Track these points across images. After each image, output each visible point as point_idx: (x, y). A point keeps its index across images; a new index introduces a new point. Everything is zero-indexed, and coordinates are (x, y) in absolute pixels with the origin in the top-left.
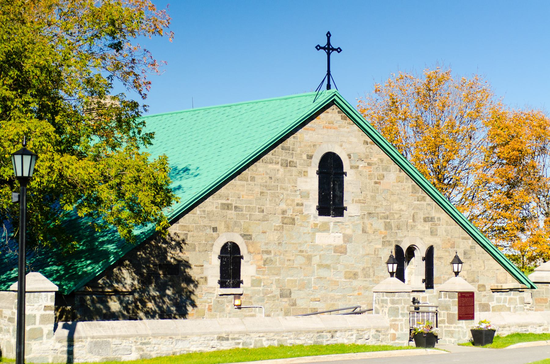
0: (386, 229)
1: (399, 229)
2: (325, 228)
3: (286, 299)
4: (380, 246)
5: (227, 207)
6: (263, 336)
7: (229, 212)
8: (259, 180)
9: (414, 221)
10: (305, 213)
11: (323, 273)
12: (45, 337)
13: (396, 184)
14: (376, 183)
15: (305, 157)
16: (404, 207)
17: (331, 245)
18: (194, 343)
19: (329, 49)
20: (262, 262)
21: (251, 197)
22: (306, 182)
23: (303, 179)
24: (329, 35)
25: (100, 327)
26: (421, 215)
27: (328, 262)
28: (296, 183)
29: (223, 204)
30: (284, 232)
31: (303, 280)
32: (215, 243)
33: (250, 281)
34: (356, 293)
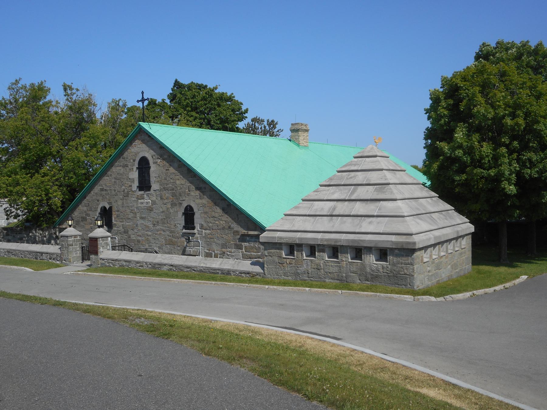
11: (142, 222)
14: (167, 170)
15: (132, 161)
23: (131, 173)
24: (143, 93)
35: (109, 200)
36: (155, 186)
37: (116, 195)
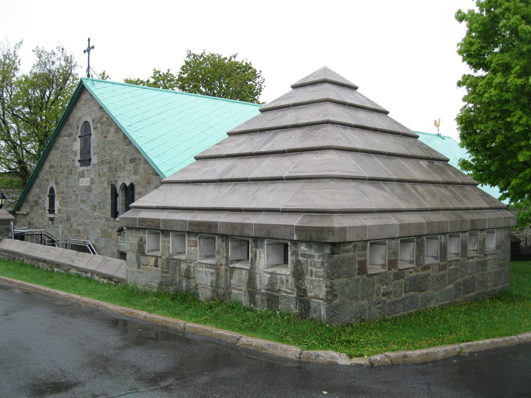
1: (116, 171)
2: (82, 175)
3: (68, 223)
8: (61, 149)
9: (124, 164)
11: (82, 206)
13: (115, 135)
15: (76, 128)
16: (119, 153)
17: (85, 186)
20: (61, 199)
24: (89, 40)
26: (128, 158)
27: (83, 199)
31: (75, 210)
35: (56, 179)
36: (94, 160)
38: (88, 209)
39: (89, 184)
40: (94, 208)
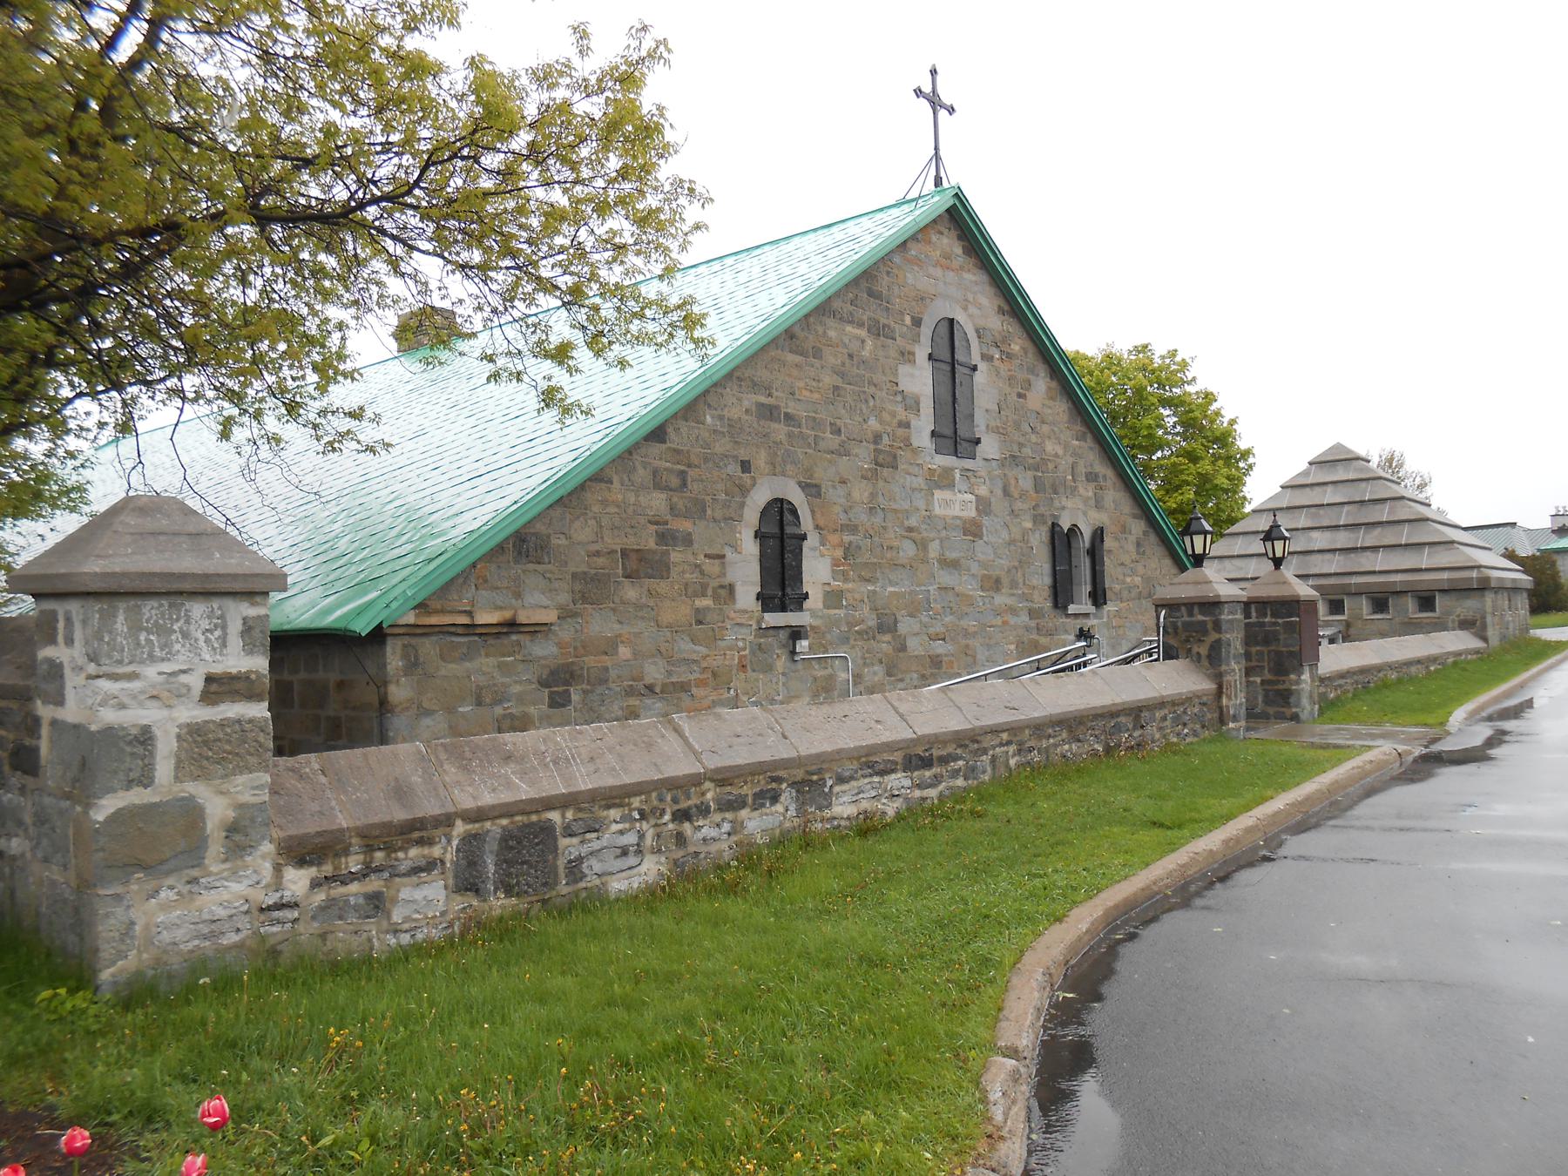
0: (1037, 492)
3: (887, 637)
4: (1029, 525)
5: (769, 413)
6: (1009, 743)
7: (775, 425)
8: (831, 359)
9: (1074, 480)
10: (915, 443)
11: (946, 578)
12: (215, 848)
15: (908, 320)
18: (845, 787)
19: (935, 102)
20: (839, 553)
21: (816, 396)
22: (912, 375)
24: (934, 72)
25: (508, 758)
26: (1082, 470)
27: (952, 555)
28: (896, 375)
29: (760, 405)
30: (881, 483)
31: (917, 593)
32: (748, 501)
33: (820, 596)
34: (998, 621)
35: (809, 471)
36: (990, 447)
37: (842, 451)
38: (969, 587)
39: (973, 514)
40: (995, 584)
